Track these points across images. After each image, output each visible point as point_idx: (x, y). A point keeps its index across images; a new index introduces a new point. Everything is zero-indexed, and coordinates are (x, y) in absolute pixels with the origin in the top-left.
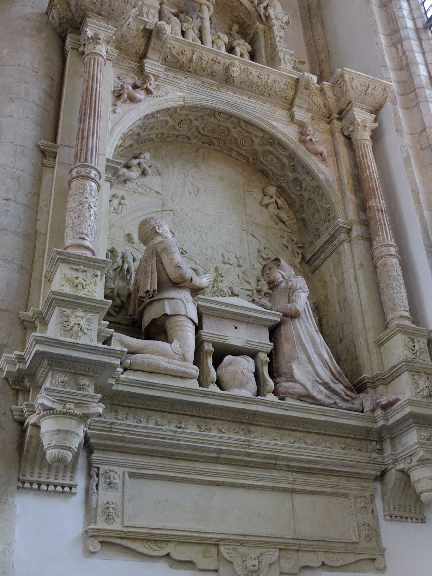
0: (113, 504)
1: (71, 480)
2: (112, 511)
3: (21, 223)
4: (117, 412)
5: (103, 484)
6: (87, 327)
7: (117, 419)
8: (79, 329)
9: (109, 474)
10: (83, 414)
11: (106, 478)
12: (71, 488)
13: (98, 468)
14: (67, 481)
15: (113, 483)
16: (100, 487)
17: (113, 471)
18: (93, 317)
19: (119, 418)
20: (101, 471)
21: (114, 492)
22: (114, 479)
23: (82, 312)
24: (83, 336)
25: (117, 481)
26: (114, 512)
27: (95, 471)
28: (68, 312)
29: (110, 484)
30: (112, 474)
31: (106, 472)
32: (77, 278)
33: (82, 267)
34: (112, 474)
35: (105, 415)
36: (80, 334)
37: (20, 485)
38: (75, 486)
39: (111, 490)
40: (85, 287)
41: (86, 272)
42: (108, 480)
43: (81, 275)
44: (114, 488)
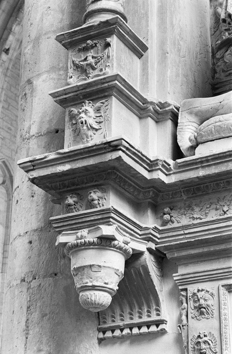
0: (205, 336)
1: (158, 315)
2: (203, 346)
3: (63, 15)
4: (193, 210)
5: (192, 311)
6: (98, 120)
7: (194, 218)
8: (85, 128)
9: (197, 296)
10: (98, 238)
11: (195, 302)
12: (157, 326)
13: (186, 290)
14: (154, 317)
15: (204, 306)
16: (190, 316)
17: (202, 290)
18: (106, 103)
19: (195, 216)
20: (190, 294)
21: (207, 319)
22: (205, 300)
23: (90, 103)
24: (95, 134)
25: (209, 303)
26: (208, 346)
27: (183, 296)
28: (75, 110)
29: (200, 309)
30: (200, 295)
31: (194, 294)
32: (85, 59)
33: (89, 42)
34: (200, 295)
35: (178, 219)
36: (90, 133)
37: (101, 335)
38: (162, 322)
39: (204, 316)
40: (96, 67)
41: (96, 46)
42: (197, 305)
43: (91, 54)
44: (208, 313)
